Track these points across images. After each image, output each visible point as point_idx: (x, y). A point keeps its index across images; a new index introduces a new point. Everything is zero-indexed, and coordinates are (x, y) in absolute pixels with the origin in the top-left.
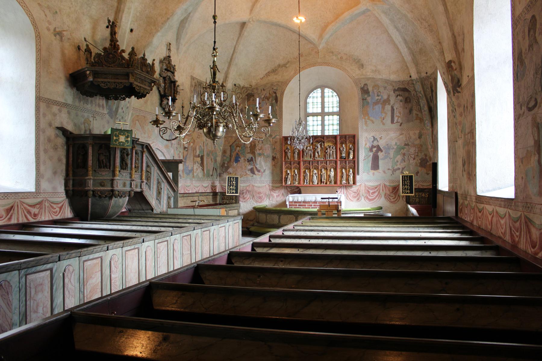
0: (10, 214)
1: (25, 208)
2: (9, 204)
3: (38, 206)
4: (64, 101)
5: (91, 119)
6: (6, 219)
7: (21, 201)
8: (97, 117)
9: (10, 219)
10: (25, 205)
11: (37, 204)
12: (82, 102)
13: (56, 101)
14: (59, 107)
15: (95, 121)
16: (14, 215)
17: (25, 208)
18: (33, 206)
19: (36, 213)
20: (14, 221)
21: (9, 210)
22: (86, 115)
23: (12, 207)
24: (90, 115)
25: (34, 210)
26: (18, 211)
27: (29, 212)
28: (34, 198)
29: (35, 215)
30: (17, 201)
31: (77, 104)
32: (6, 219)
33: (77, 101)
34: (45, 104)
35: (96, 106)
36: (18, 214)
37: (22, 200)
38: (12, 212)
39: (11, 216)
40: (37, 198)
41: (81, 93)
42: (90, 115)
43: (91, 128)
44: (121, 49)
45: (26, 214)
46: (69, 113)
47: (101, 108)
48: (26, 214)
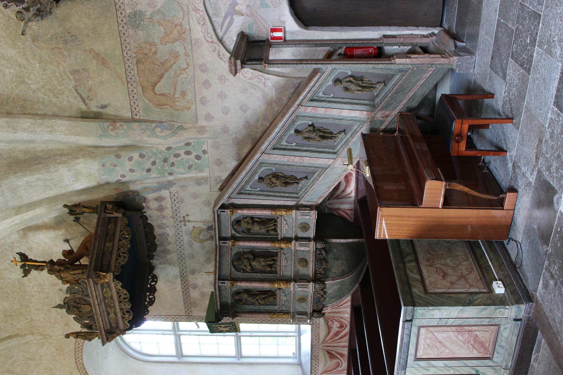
0: (337, 355)
1: (331, 339)
2: (325, 355)
3: (330, 323)
4: (179, 279)
5: (190, 226)
6: (341, 359)
7: (322, 343)
8: (183, 214)
9: (342, 355)
10: (327, 339)
11: (327, 324)
12: (169, 247)
13: (183, 292)
14: (191, 289)
15: (191, 218)
16: (338, 351)
17: (331, 339)
18: (329, 329)
19: (338, 326)
20: (345, 352)
21: (331, 356)
22: (186, 238)
23: (328, 352)
24: (184, 228)
25: (335, 327)
26: (334, 346)
27: (337, 334)
28: (318, 328)
29: (342, 326)
30: (321, 346)
31: (173, 257)
32: (341, 359)
33: (169, 256)
34: (192, 308)
35: (164, 217)
36: (337, 346)
37: (321, 342)
38: (334, 353)
39: (338, 353)
40: (319, 324)
41: (155, 250)
42: (184, 228)
43: (205, 227)
44: (63, 258)
45: (338, 337)
46: (193, 272)
47: (163, 203)
48: (338, 337)
